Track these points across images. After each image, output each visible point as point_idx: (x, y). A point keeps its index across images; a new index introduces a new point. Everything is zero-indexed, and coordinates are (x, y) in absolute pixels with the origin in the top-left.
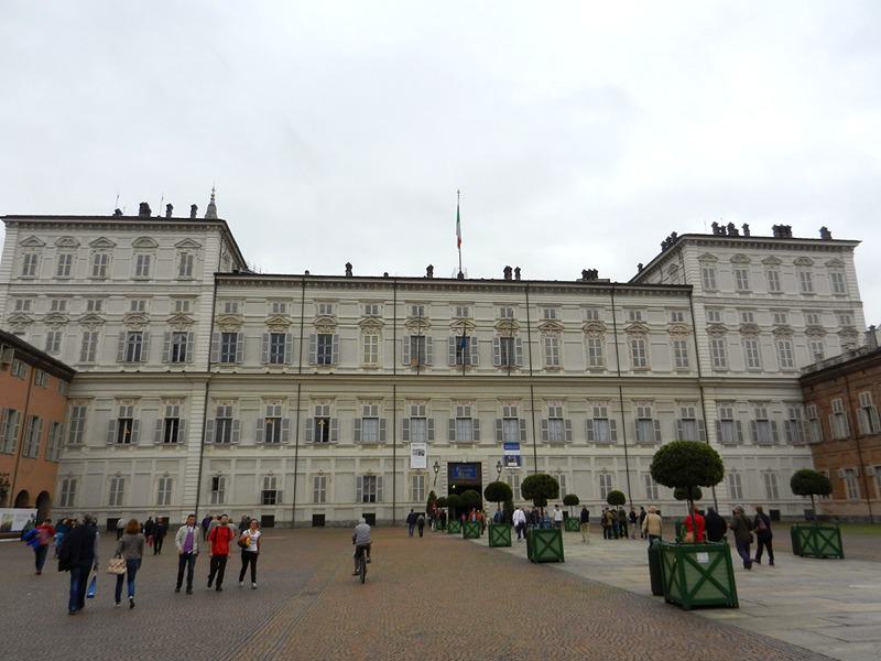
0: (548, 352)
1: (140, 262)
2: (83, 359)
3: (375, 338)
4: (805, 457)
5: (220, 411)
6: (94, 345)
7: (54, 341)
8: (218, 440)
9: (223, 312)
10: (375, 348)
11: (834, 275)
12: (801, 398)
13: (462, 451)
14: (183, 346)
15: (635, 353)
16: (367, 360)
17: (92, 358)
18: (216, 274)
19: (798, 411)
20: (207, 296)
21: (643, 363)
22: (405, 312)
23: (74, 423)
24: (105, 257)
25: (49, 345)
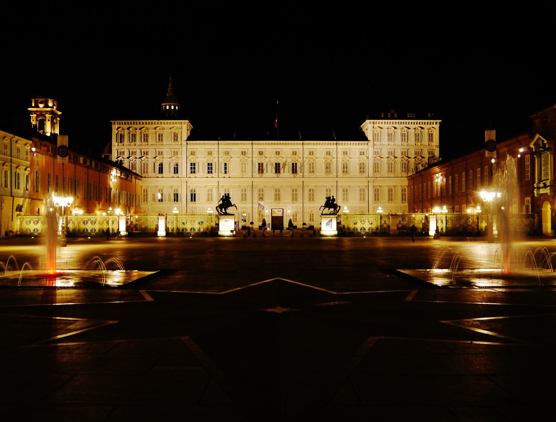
0: (310, 168)
1: (159, 136)
2: (144, 173)
3: (245, 164)
4: (405, 207)
5: (192, 191)
6: (147, 168)
7: (134, 166)
8: (192, 200)
9: (190, 153)
10: (245, 168)
11: (429, 134)
12: (407, 184)
13: (276, 205)
14: (177, 168)
15: (344, 168)
16: (242, 172)
17: (147, 172)
18: (187, 140)
19: (405, 190)
20: (184, 148)
21: (347, 172)
22: (256, 154)
23: (144, 195)
24: (147, 135)
25: (132, 168)
